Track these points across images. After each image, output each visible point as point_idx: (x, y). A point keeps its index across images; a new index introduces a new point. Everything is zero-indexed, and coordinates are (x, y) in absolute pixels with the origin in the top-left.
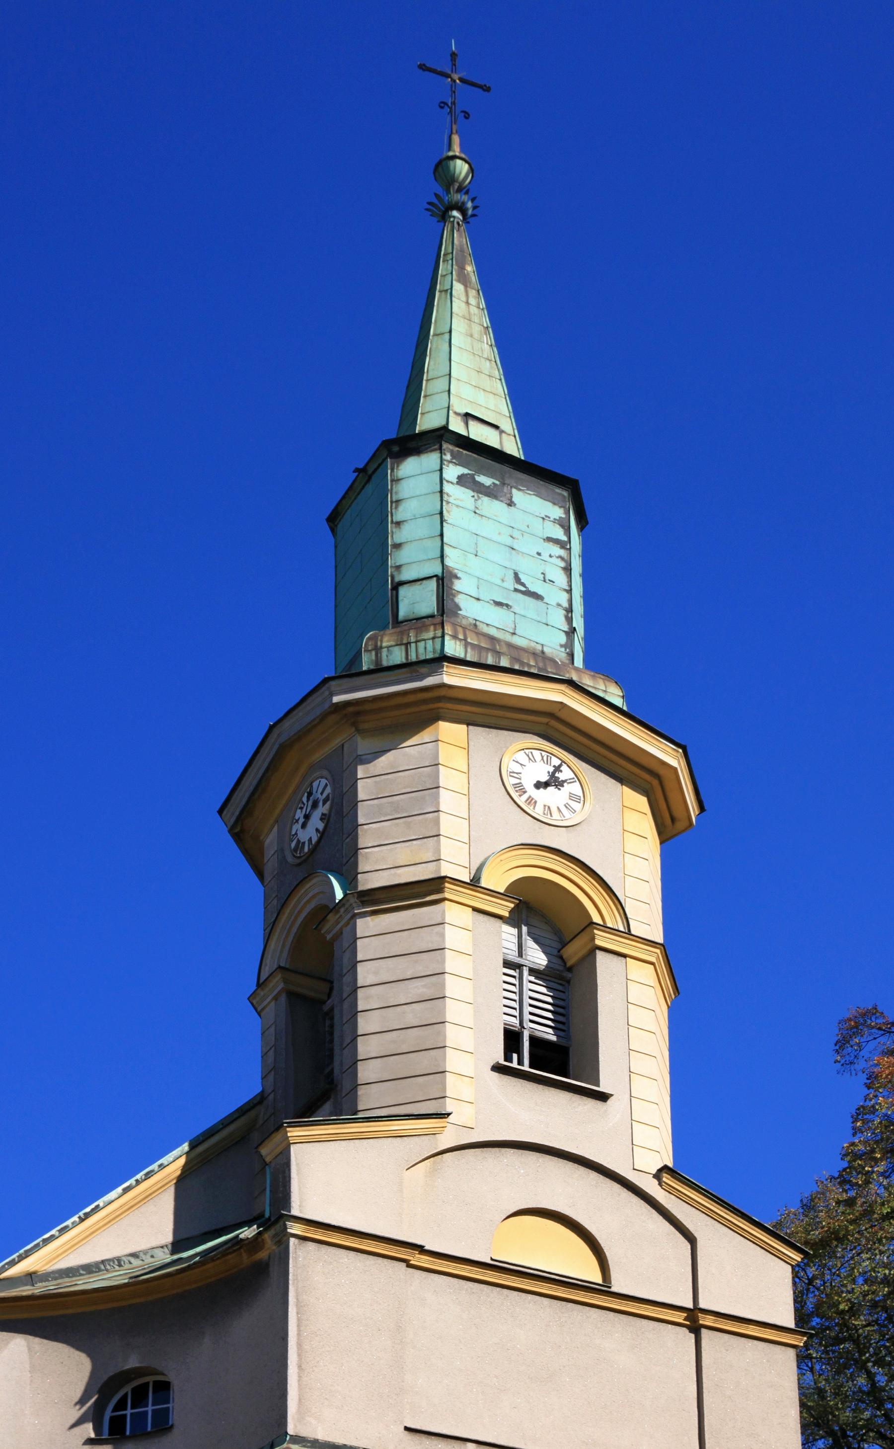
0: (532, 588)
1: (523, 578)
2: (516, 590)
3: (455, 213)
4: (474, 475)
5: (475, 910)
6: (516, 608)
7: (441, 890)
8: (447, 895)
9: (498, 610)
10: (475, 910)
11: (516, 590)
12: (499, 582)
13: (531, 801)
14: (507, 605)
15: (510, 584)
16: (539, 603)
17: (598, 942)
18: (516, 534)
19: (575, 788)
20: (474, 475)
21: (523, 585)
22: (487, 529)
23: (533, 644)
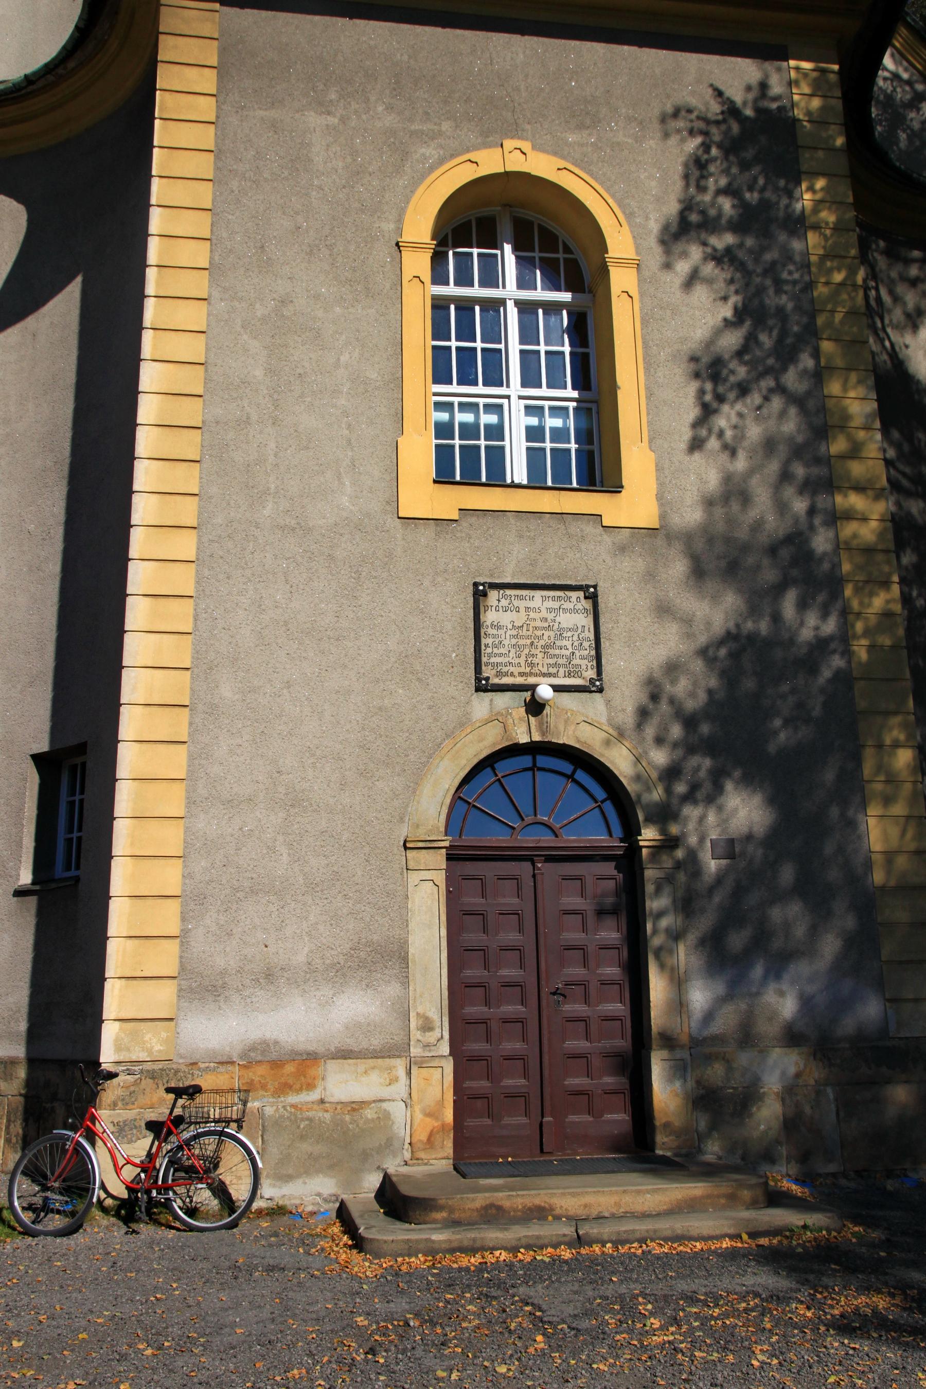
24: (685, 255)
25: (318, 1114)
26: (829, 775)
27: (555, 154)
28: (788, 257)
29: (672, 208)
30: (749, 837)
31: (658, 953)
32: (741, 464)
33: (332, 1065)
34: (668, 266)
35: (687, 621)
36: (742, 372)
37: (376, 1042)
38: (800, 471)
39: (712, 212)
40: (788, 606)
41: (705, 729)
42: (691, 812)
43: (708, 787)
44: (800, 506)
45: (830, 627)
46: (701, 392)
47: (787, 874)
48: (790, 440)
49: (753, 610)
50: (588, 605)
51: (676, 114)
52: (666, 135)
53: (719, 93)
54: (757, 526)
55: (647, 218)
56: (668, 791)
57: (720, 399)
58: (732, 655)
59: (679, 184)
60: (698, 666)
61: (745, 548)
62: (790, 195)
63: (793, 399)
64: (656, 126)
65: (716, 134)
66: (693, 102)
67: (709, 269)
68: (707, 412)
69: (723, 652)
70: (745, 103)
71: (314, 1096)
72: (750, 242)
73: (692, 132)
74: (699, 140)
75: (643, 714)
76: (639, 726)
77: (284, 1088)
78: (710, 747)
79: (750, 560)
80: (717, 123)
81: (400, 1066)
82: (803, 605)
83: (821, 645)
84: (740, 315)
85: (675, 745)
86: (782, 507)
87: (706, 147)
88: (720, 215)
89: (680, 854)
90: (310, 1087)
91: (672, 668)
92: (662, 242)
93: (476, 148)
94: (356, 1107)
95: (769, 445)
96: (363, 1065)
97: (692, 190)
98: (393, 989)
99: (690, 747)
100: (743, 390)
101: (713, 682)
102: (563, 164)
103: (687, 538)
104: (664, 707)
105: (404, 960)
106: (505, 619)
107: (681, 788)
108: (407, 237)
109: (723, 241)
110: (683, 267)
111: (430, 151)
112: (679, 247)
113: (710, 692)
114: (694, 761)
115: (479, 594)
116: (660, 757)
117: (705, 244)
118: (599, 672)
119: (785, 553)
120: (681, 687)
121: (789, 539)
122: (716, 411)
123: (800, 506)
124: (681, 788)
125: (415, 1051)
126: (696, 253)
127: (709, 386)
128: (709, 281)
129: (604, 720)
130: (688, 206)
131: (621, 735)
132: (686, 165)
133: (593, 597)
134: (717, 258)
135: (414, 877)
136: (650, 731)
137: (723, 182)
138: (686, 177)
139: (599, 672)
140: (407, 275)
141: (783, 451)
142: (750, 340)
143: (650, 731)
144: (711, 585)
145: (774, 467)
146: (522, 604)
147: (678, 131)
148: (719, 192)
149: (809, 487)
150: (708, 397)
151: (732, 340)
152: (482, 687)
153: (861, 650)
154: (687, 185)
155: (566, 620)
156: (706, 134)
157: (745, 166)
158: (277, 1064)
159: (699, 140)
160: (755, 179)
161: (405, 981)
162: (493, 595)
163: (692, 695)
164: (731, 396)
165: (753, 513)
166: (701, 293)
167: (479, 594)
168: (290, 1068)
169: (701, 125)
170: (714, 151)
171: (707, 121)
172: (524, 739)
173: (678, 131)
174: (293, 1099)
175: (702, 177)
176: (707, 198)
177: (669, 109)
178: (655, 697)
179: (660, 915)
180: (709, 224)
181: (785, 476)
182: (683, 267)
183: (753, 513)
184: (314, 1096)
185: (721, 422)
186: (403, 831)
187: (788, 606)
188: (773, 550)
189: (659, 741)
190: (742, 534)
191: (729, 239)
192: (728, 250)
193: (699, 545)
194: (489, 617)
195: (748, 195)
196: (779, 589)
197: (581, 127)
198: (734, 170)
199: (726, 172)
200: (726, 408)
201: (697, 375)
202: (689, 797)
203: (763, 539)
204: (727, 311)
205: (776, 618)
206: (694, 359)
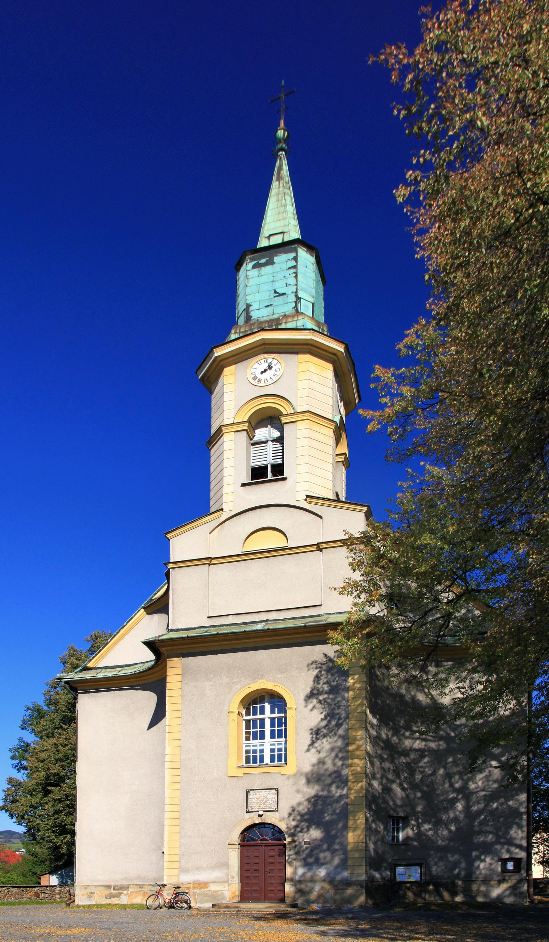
0: (281, 292)
1: (277, 291)
2: (274, 297)
3: (280, 153)
4: (258, 262)
5: (235, 432)
6: (275, 304)
7: (222, 431)
8: (224, 432)
9: (268, 309)
10: (235, 432)
11: (274, 297)
12: (268, 298)
13: (260, 380)
14: (271, 305)
15: (273, 294)
16: (285, 296)
17: (283, 422)
18: (275, 274)
19: (278, 366)
20: (258, 262)
21: (278, 293)
22: (264, 279)
23: (281, 314)
24: (312, 702)
25: (208, 893)
26: (340, 825)
27: (274, 681)
28: (343, 698)
29: (308, 690)
30: (315, 840)
31: (289, 863)
32: (322, 755)
33: (211, 885)
34: (306, 706)
35: (304, 793)
36: (325, 731)
37: (221, 880)
38: (340, 755)
39: (321, 690)
40: (333, 788)
41: (306, 817)
42: (300, 834)
43: (305, 830)
44: (340, 763)
45: (345, 792)
46: (313, 737)
47: (325, 846)
48: (338, 747)
49: (323, 790)
50: (276, 792)
51: (312, 663)
52: (309, 670)
53: (326, 655)
54: (326, 770)
55: (300, 695)
56: (295, 830)
57: (317, 739)
58: (315, 800)
59: (312, 683)
60: (306, 803)
61: (323, 775)
62: (346, 681)
63: (340, 736)
64: (306, 668)
65: (324, 667)
66: (317, 659)
67: (318, 705)
68: (313, 743)
69: (313, 800)
70: (334, 657)
71: (208, 889)
72: (331, 696)
73: (316, 668)
74: (318, 670)
75: (290, 814)
76: (289, 817)
77: (201, 888)
78: (306, 820)
79: (324, 778)
80: (325, 664)
81: (226, 885)
82: (338, 787)
83: (341, 797)
84: (326, 717)
85: (298, 821)
86: (334, 764)
87: (320, 672)
88: (323, 690)
89: (297, 843)
90: (207, 888)
91: (299, 804)
92: (305, 700)
93: (251, 684)
94: (216, 892)
95: (332, 749)
96: (218, 884)
97: (316, 684)
98: (226, 871)
99: (301, 821)
100: (325, 736)
101: (309, 806)
102: (275, 684)
103: (306, 775)
104: (296, 812)
105: (228, 865)
106: (254, 797)
107: (299, 829)
108: (230, 710)
109: (321, 698)
110: (310, 706)
111: (238, 686)
112: (310, 700)
113: (308, 809)
114: (303, 824)
115: (248, 792)
116: (294, 823)
117: (317, 699)
118: (278, 807)
119: (333, 776)
120: (301, 808)
121: (335, 772)
122: (316, 742)
123: (340, 763)
124: (299, 829)
125: (230, 882)
126: (315, 701)
127: (314, 736)
128: (318, 709)
129: (278, 817)
130: (313, 689)
131: (283, 819)
132: (314, 678)
133: (277, 791)
134: (320, 702)
135: (230, 850)
136: (291, 818)
137: (325, 680)
138: (314, 681)
139: (278, 807)
140: (231, 720)
141: (337, 750)
142: (329, 722)
143: (291, 818)
144: (311, 784)
145: (333, 755)
146: (259, 794)
147: (313, 668)
148: (324, 684)
149: (343, 759)
150: (314, 739)
151: (324, 723)
152: (248, 812)
153: (352, 796)
154: (314, 683)
155: (269, 796)
156: (320, 668)
157: (332, 675)
158: (200, 884)
159: (318, 670)
160: (335, 679)
161: (228, 869)
162: (251, 792)
163: (303, 810)
164: (321, 738)
165: (326, 767)
166: (315, 711)
167: (248, 792)
168: (202, 885)
169: (320, 665)
170: (323, 672)
171: (322, 664)
172: (257, 822)
173: (313, 668)
174: (203, 890)
175: (318, 680)
176: (319, 686)
177: (310, 662)
178: (293, 811)
179: (289, 855)
180: (320, 693)
181: (337, 756)
182: (310, 706)
183: (326, 767)
184: (208, 889)
185: (316, 745)
186: (228, 841)
187: (333, 788)
188: (330, 775)
189: (294, 820)
190: (322, 772)
191: (326, 696)
192: (324, 699)
193: (310, 776)
194: (249, 797)
195: (333, 683)
196: (330, 785)
197: (282, 673)
198: (330, 676)
199: (326, 678)
200: (319, 741)
201: (311, 734)
202: (301, 831)
203: (328, 773)
204: (322, 716)
205: (329, 791)
206: (311, 729)
